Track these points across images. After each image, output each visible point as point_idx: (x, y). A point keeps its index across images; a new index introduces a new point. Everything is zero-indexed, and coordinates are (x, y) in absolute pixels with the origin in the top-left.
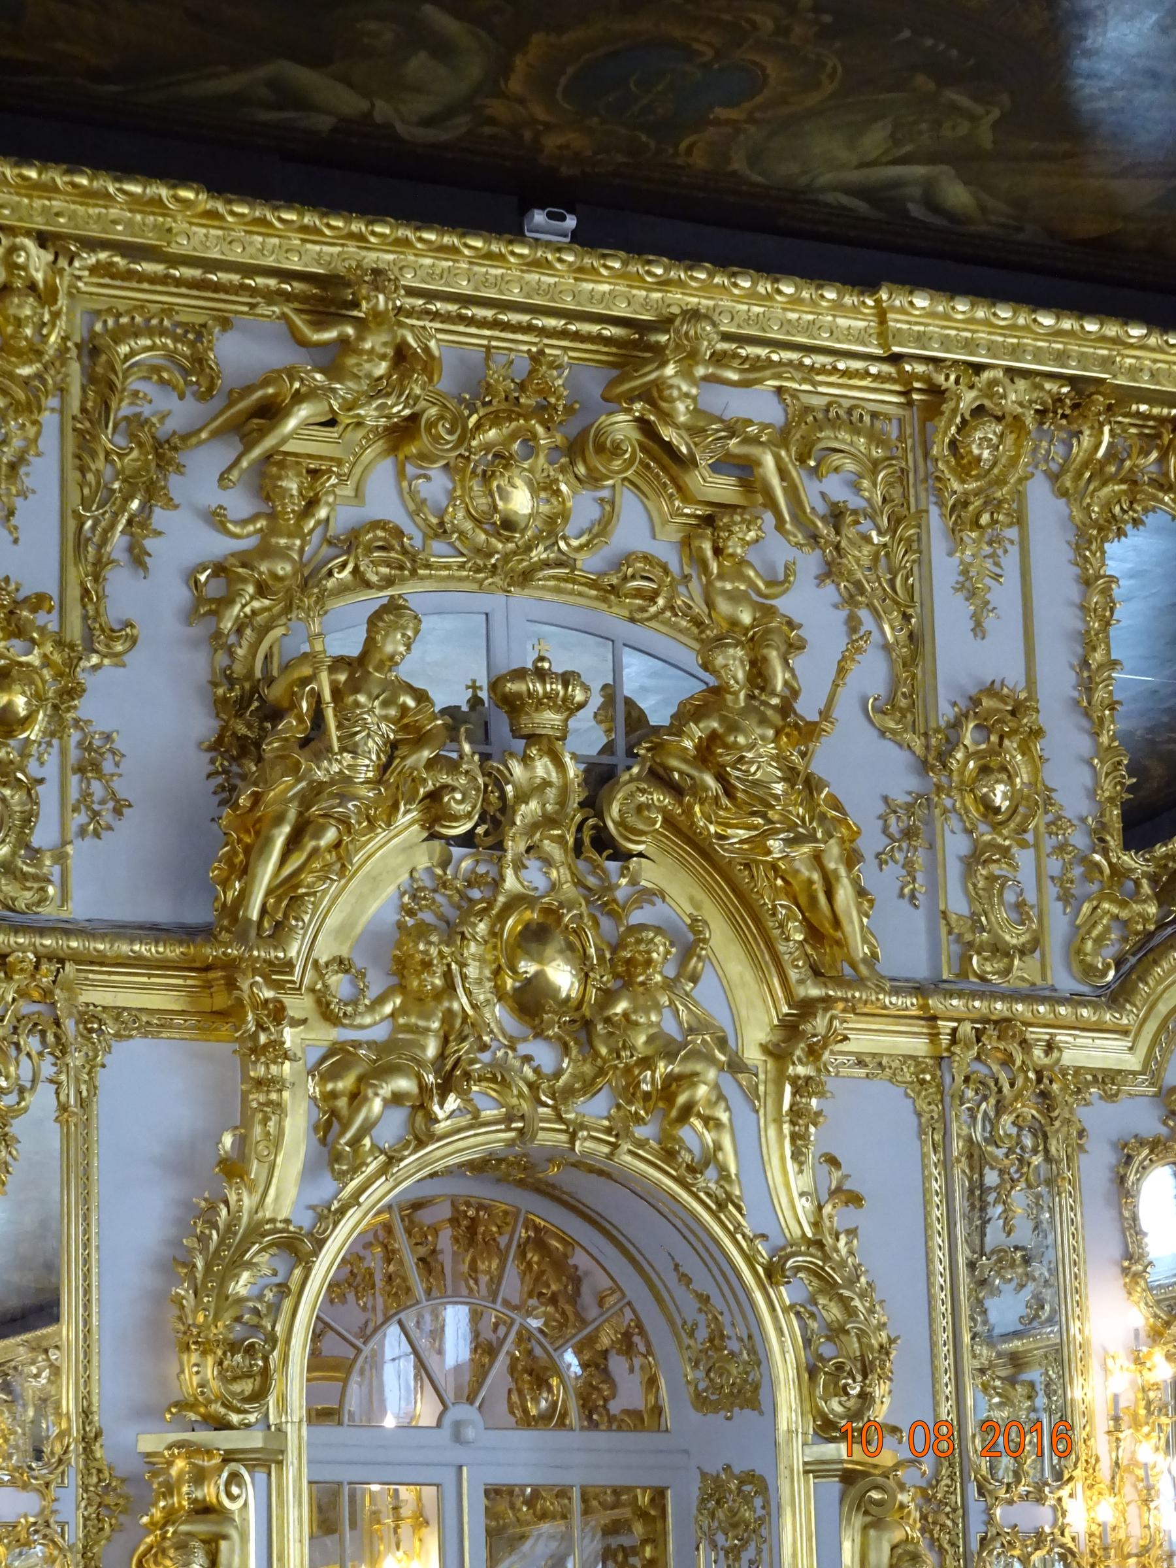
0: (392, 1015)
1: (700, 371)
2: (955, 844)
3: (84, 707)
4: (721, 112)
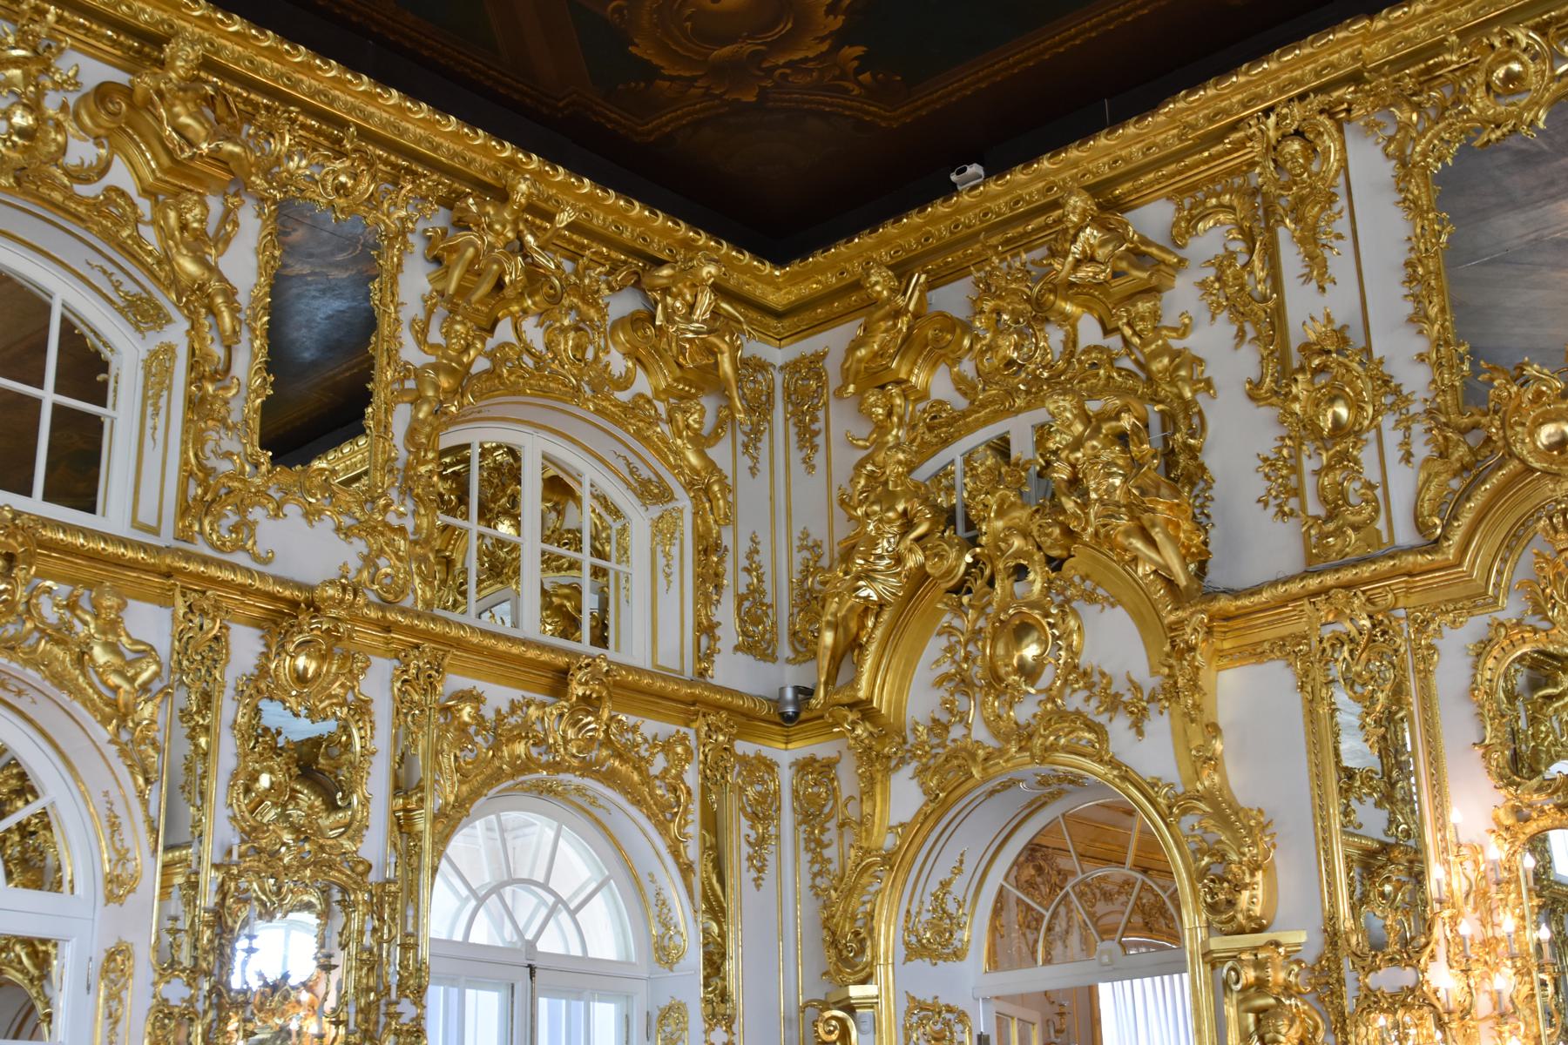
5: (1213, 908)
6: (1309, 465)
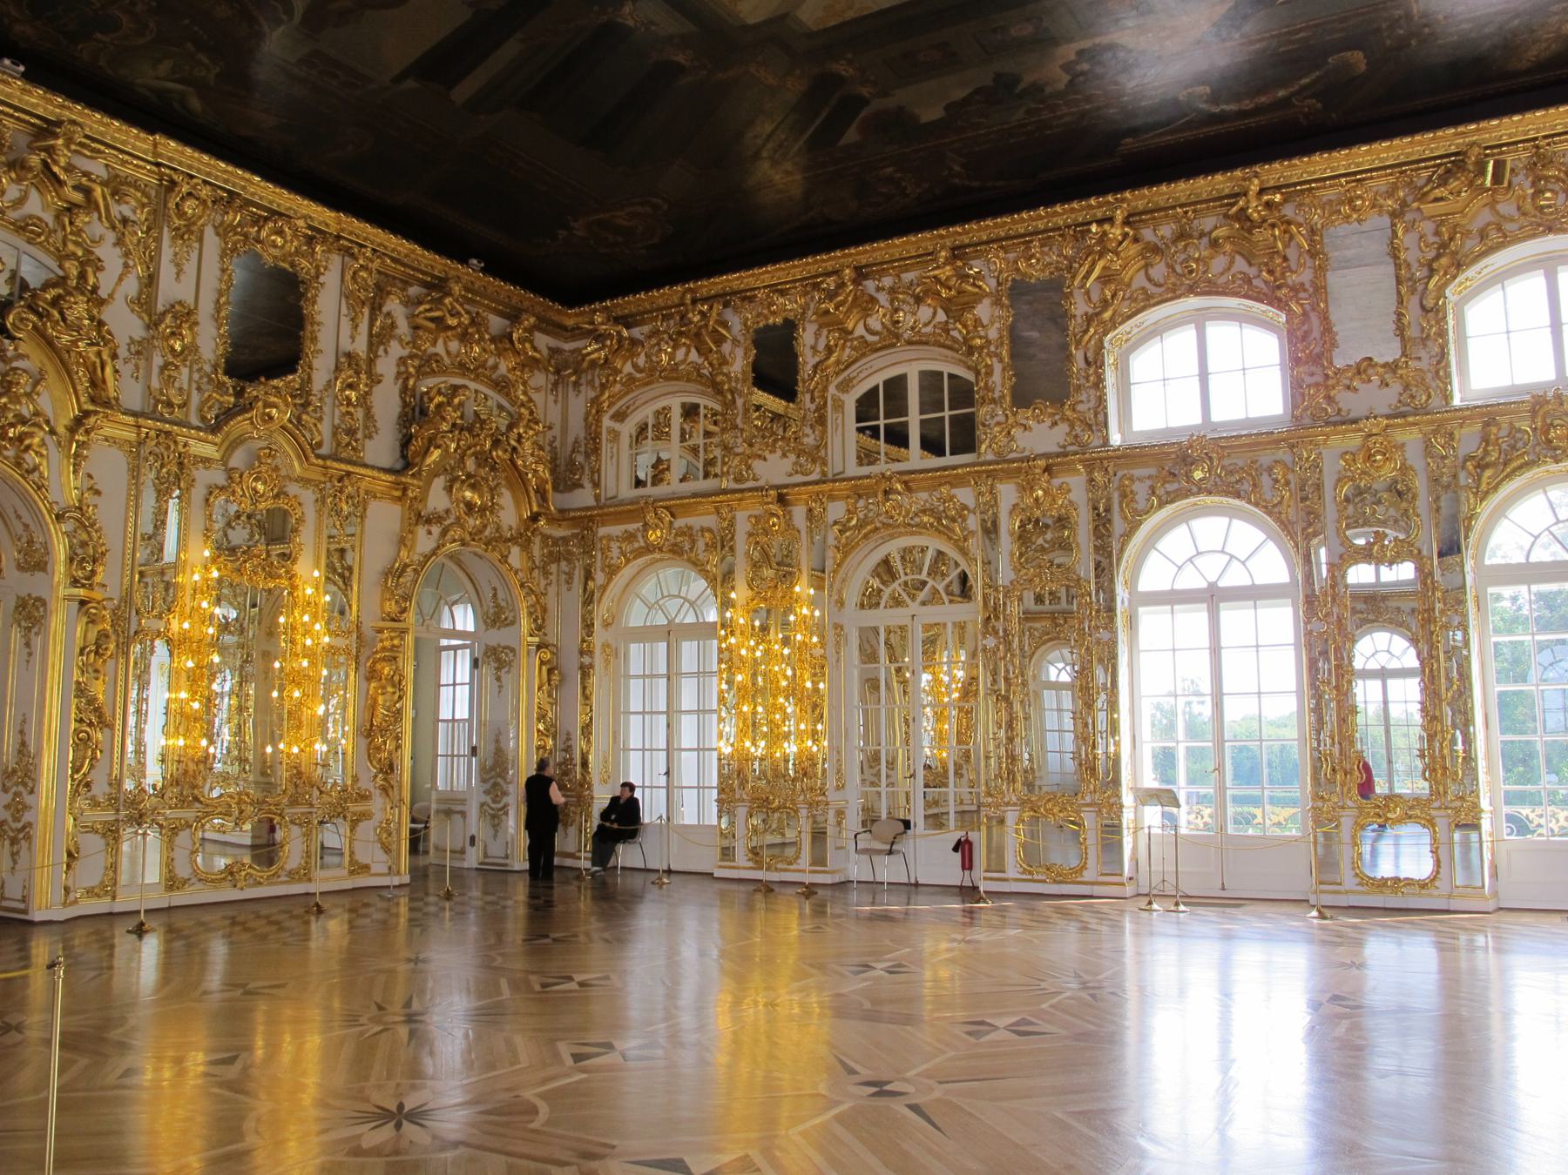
1: (73, 147)
2: (158, 361)
4: (98, 35)
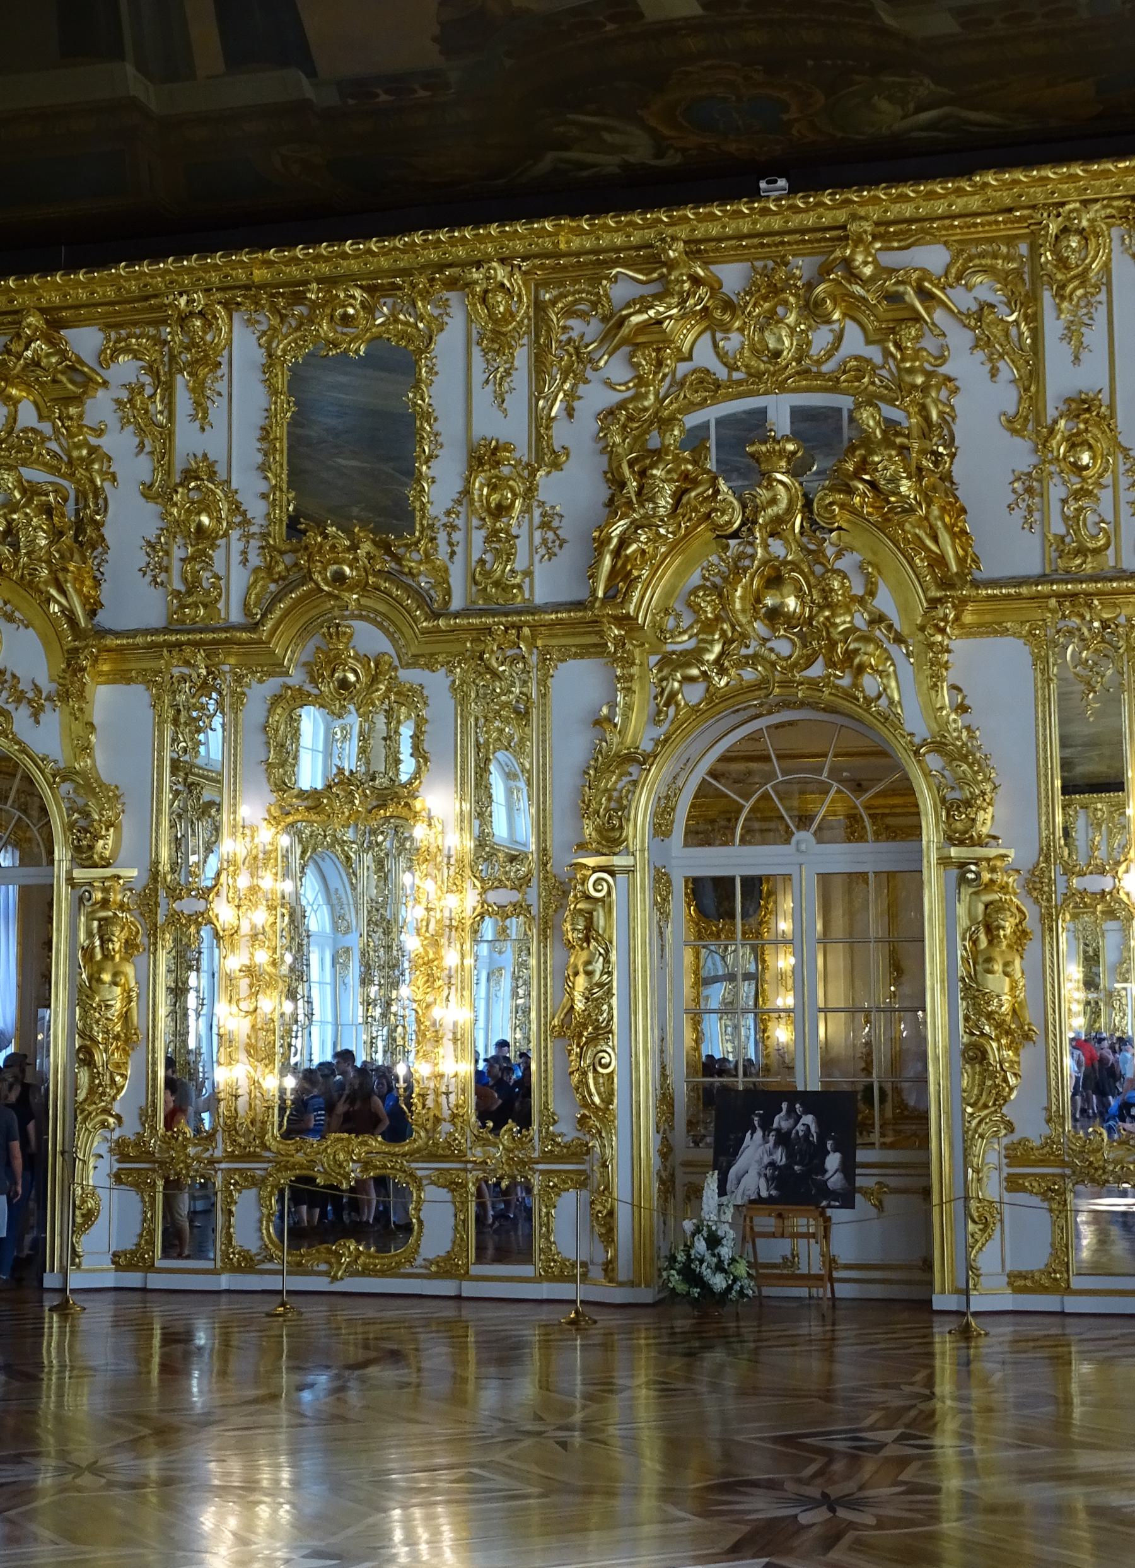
0: (697, 635)
3: (541, 495)
5: (78, 849)
6: (177, 553)
